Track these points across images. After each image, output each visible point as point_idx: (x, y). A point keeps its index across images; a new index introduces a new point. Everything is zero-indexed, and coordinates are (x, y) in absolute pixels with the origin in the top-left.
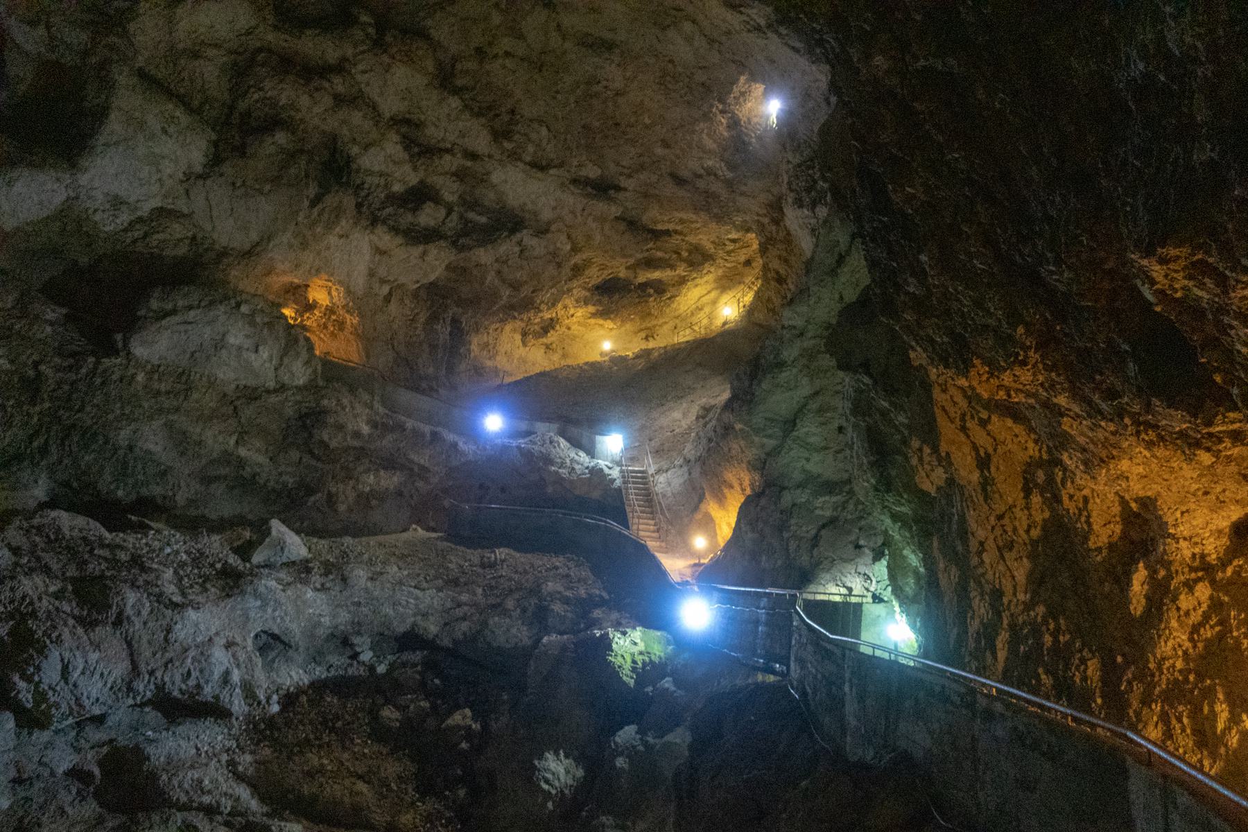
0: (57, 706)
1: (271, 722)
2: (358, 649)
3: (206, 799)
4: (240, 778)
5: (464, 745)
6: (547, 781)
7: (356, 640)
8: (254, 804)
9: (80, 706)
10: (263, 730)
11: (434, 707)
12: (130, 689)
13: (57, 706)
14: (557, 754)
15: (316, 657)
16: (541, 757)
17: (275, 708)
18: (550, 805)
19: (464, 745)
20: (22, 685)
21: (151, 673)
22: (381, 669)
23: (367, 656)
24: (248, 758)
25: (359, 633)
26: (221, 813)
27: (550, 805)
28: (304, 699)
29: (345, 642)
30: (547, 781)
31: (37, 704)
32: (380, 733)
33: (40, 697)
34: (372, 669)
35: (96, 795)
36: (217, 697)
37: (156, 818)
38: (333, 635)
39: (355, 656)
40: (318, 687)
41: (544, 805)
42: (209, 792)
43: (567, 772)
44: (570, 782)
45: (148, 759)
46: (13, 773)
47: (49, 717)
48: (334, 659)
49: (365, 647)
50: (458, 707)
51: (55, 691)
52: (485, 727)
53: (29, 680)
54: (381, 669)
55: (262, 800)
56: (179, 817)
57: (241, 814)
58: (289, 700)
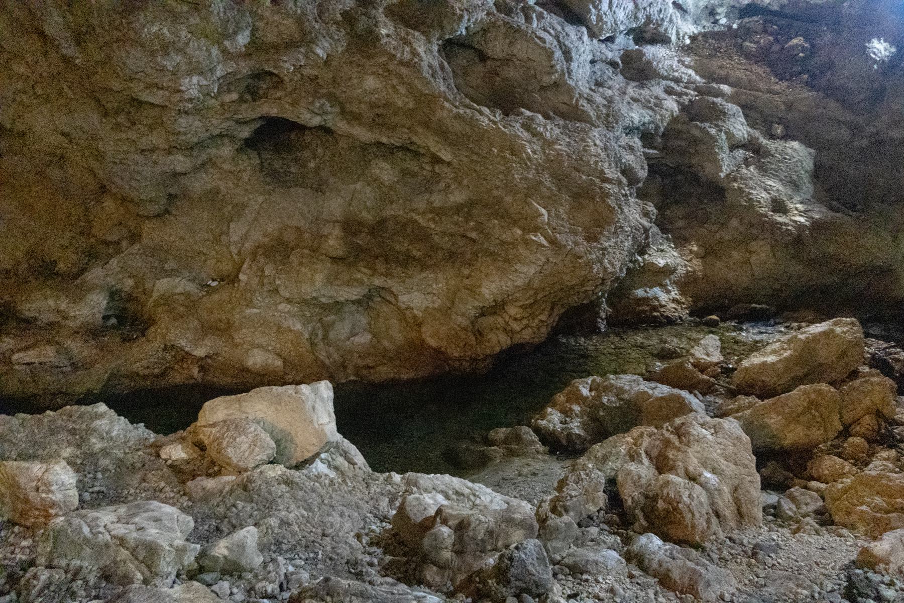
0: (606, 22)
1: (688, 46)
2: (718, 17)
3: (676, 74)
4: (688, 67)
5: (801, 55)
6: (874, 53)
7: (719, 10)
8: (698, 78)
9: (616, 24)
10: (687, 50)
11: (777, 40)
12: (636, 18)
13: (606, 22)
14: (879, 40)
15: (696, 22)
16: (869, 41)
17: (688, 42)
18: (875, 67)
19: (801, 55)
20: (593, 10)
21: (645, 9)
22: (735, 26)
23: (723, 21)
24: (689, 59)
25: (721, 6)
26: (682, 82)
27: (875, 67)
28: (700, 38)
29: (711, 12)
30: (874, 53)
31: (597, 24)
32: (748, 55)
33: (600, 18)
34: (729, 27)
35: (622, 73)
36: (666, 30)
37: (653, 83)
38: (706, 7)
39: (716, 22)
40: (705, 35)
41: (871, 68)
42: (677, 71)
43: (886, 49)
44: (887, 54)
45: (644, 55)
46: (590, 58)
47: (601, 29)
48: (704, 23)
49: (723, 15)
50: (796, 36)
51: (605, 14)
52: (812, 46)
53: (596, 7)
54: (735, 26)
55: (701, 76)
56: (664, 82)
57: (692, 83)
58: (693, 38)
